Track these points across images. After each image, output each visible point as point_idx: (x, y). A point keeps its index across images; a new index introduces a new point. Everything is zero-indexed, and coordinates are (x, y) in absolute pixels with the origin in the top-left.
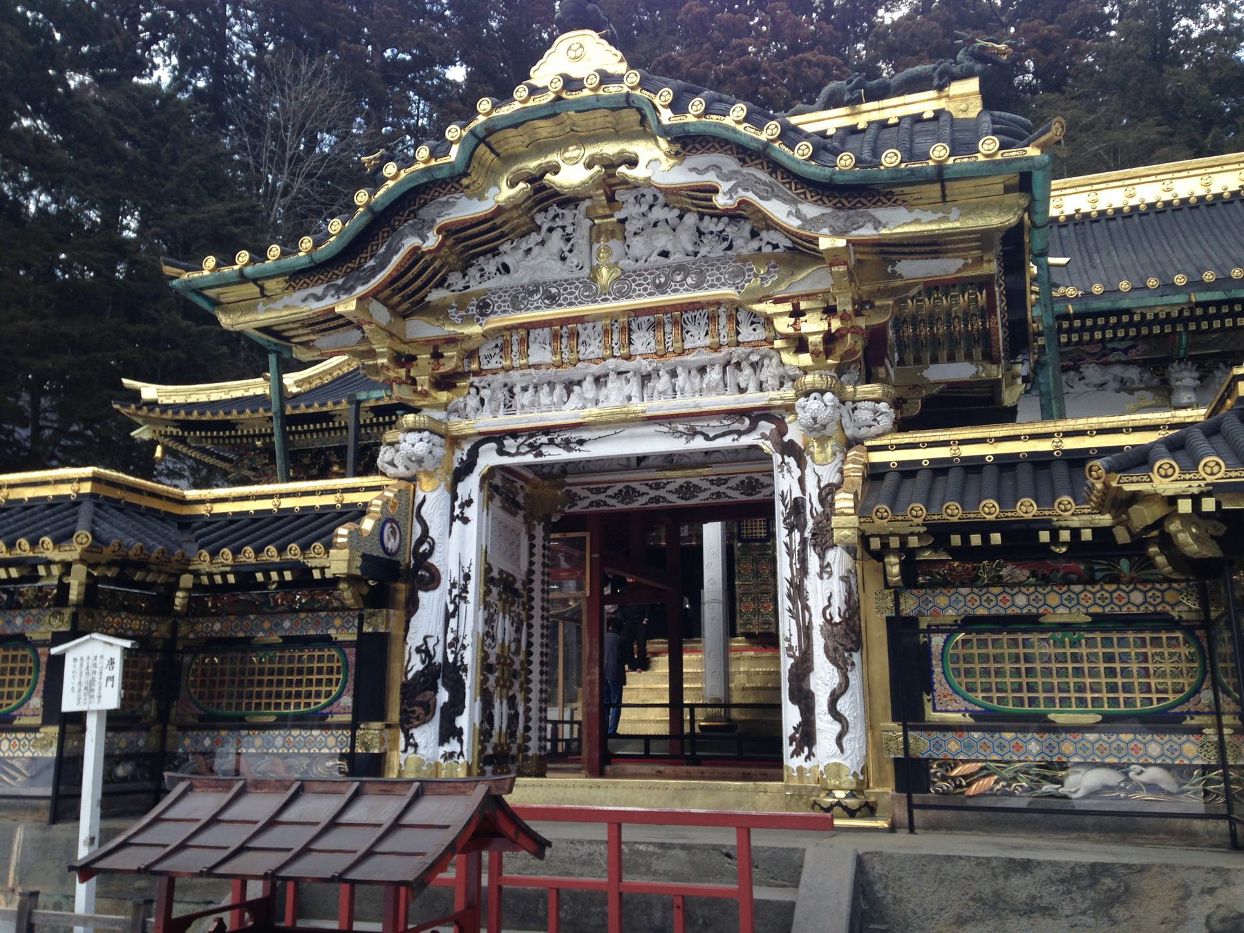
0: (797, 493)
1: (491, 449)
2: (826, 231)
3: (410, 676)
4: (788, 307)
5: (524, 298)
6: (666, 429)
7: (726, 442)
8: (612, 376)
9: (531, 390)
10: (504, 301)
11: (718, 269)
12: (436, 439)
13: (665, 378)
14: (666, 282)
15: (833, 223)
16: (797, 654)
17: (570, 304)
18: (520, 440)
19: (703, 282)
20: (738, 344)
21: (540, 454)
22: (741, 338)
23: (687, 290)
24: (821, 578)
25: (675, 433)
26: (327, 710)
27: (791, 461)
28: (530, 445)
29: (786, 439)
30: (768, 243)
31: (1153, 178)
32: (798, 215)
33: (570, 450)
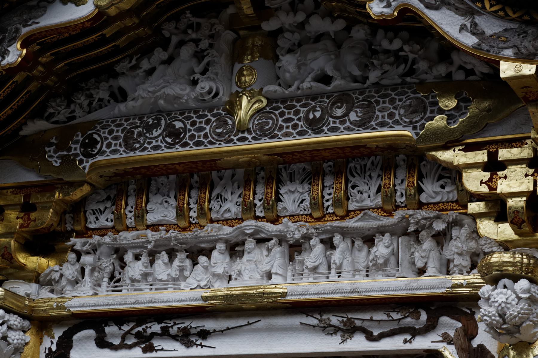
1: (88, 338)
5: (140, 134)
6: (314, 322)
8: (250, 244)
9: (145, 259)
10: (116, 138)
11: (392, 101)
12: (14, 320)
13: (319, 249)
14: (322, 118)
17: (198, 144)
18: (126, 328)
19: (370, 119)
20: (421, 205)
22: (423, 198)
23: (348, 129)
28: (138, 335)
29: (475, 343)
30: (461, 68)
32: (475, 31)
33: (189, 344)
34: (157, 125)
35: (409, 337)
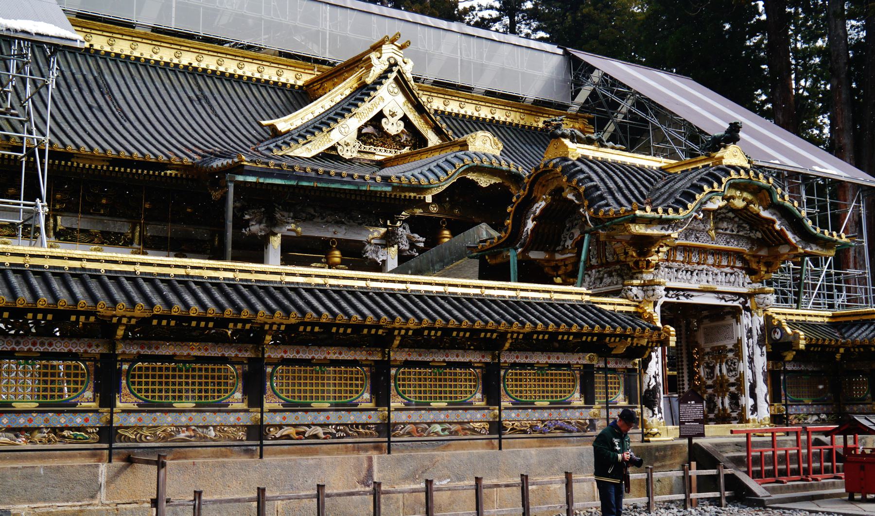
3: (651, 387)
4: (757, 260)
7: (730, 303)
21: (678, 299)
25: (718, 298)
27: (749, 314)
29: (747, 305)
31: (457, 99)
33: (687, 298)
34: (692, 234)
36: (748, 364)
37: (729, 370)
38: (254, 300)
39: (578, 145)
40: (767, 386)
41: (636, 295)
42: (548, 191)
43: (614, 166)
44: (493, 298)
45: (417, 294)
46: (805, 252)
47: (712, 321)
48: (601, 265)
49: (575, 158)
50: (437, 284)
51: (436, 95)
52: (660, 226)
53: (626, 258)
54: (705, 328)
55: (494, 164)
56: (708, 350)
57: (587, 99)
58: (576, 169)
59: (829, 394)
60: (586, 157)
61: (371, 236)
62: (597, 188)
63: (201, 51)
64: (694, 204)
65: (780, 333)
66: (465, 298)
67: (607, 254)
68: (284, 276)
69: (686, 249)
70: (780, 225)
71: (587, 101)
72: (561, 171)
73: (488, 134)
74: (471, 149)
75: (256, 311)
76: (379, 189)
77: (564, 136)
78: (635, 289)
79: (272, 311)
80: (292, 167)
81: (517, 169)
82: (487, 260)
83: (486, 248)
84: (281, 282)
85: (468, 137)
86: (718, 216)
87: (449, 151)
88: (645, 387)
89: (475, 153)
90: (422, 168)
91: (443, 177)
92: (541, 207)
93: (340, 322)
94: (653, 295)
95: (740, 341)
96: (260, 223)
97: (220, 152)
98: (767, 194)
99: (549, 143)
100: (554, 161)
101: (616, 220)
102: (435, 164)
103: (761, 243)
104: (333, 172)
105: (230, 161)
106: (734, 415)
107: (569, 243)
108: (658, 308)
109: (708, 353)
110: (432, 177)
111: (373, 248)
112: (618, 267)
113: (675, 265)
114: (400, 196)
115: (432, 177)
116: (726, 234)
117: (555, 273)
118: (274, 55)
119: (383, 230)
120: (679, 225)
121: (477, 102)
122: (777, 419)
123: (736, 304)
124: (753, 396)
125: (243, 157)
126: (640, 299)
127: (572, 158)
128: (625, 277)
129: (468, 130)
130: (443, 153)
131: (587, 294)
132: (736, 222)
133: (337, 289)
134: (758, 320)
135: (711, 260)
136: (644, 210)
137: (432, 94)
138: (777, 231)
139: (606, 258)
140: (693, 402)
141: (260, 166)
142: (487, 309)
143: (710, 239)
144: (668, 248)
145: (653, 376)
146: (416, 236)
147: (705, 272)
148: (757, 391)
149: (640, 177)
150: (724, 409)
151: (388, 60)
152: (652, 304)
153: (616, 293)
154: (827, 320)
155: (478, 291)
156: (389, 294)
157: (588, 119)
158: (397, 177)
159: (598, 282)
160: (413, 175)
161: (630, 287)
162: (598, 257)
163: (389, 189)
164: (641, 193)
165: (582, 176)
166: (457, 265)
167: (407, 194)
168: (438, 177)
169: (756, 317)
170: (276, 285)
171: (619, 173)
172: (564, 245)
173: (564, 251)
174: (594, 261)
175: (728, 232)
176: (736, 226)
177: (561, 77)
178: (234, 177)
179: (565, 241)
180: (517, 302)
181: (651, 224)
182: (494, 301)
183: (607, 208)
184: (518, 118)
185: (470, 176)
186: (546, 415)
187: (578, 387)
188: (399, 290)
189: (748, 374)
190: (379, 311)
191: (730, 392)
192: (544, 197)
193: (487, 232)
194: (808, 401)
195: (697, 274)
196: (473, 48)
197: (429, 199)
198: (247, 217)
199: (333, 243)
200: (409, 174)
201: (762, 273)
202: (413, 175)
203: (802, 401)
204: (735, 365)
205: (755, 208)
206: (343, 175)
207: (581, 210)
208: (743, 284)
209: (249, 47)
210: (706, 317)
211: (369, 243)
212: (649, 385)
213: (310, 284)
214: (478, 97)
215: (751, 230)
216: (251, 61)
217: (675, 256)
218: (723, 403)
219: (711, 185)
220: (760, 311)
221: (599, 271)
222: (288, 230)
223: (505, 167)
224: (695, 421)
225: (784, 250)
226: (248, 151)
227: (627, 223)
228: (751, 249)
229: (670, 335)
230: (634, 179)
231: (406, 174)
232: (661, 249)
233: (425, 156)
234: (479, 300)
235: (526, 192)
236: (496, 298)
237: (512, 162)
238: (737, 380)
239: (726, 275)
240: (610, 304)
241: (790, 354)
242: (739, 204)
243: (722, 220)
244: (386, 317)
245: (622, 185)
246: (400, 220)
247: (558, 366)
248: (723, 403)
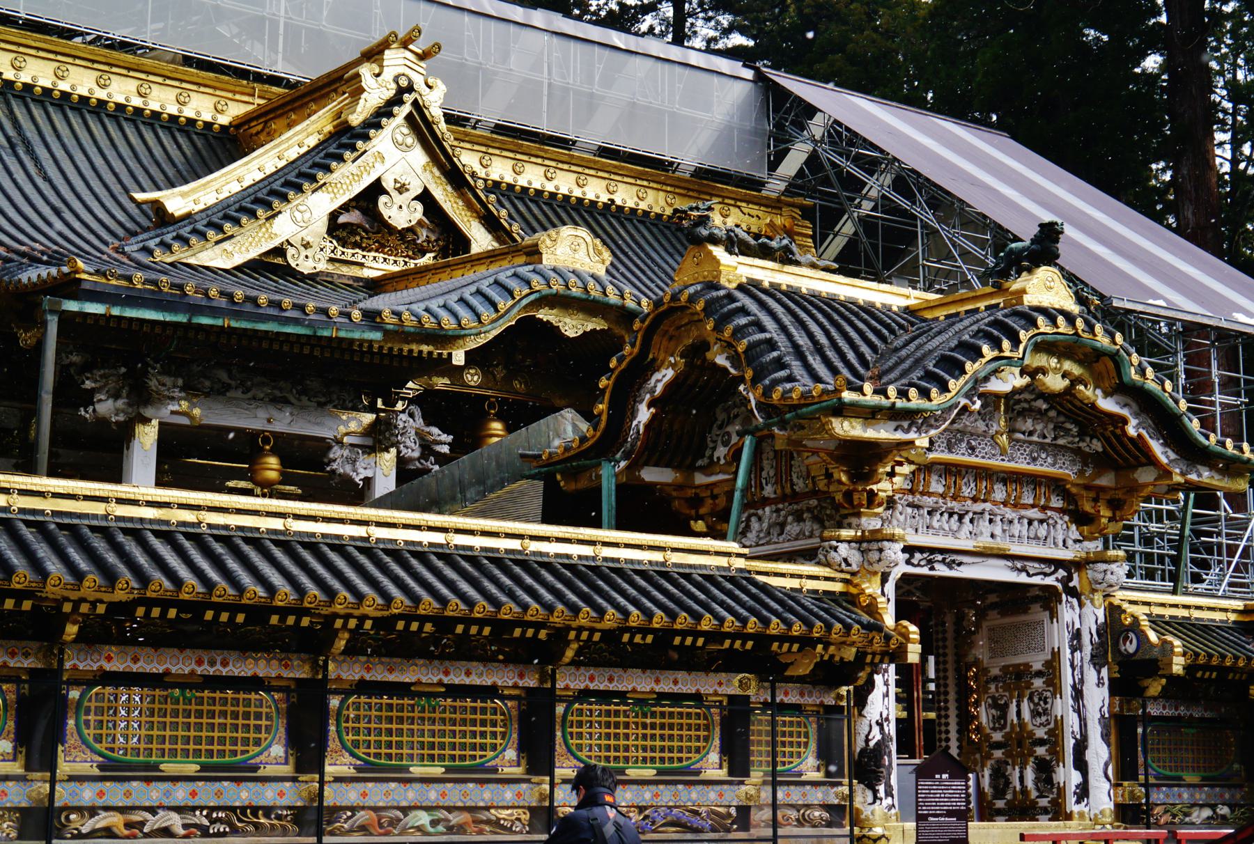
0: (1077, 626)
2: (1178, 471)
3: (872, 744)
4: (1092, 494)
7: (1037, 580)
15: (1181, 466)
16: (1078, 737)
17: (983, 457)
21: (932, 569)
24: (1098, 686)
25: (1014, 569)
26: (257, 760)
27: (1075, 601)
29: (1071, 584)
31: (539, 161)
33: (951, 568)
34: (961, 441)
35: (1042, 576)
36: (1071, 702)
37: (1035, 714)
38: (43, 551)
39: (742, 259)
40: (1109, 745)
41: (845, 560)
42: (681, 348)
43: (811, 303)
44: (546, 559)
45: (389, 546)
46: (1187, 482)
47: (1003, 614)
48: (783, 498)
49: (734, 285)
50: (431, 529)
51: (497, 152)
52: (894, 424)
53: (828, 485)
54: (991, 629)
55: (593, 293)
56: (995, 671)
57: (801, 169)
58: (733, 306)
59: (1236, 766)
60: (756, 284)
61: (342, 429)
62: (771, 344)
63: (22, 49)
64: (962, 381)
65: (1135, 641)
66: (487, 558)
67: (794, 476)
68: (113, 504)
69: (951, 471)
70: (1137, 427)
71: (800, 173)
72: (704, 310)
73: (583, 232)
74: (548, 260)
75: (44, 574)
76: (357, 335)
77: (714, 240)
78: (843, 549)
79: (79, 575)
80: (181, 287)
81: (639, 304)
82: (558, 482)
83: (556, 459)
84: (106, 517)
85: (543, 239)
86: (1015, 404)
87: (505, 264)
88: (860, 744)
89: (554, 270)
90: (447, 297)
91: (487, 314)
92: (665, 380)
93: (220, 600)
94: (880, 560)
95: (1056, 655)
96: (116, 396)
97: (43, 253)
98: (1111, 365)
99: (686, 248)
100: (692, 290)
101: (804, 410)
102: (473, 288)
103: (1101, 462)
104: (263, 299)
105: (54, 271)
106: (1044, 802)
107: (721, 452)
108: (890, 588)
109: (995, 679)
110: (465, 315)
111: (346, 453)
112: (814, 502)
113: (929, 501)
114: (401, 350)
115: (465, 315)
116: (1031, 443)
117: (693, 512)
118: (173, 62)
119: (368, 418)
120: (932, 422)
121: (580, 169)
122: (1128, 813)
123: (1050, 581)
124: (1081, 765)
125: (80, 264)
126: (855, 568)
127: (727, 285)
128: (827, 524)
129: (535, 224)
130: (494, 268)
131: (739, 555)
132: (1051, 420)
133: (223, 533)
134: (1095, 614)
135: (999, 493)
136: (860, 390)
137: (491, 151)
138: (1131, 439)
139: (792, 484)
140: (945, 776)
141: (114, 282)
142: (529, 580)
143: (998, 451)
144: (913, 467)
145: (877, 723)
146: (435, 430)
147: (987, 517)
148: (1090, 756)
149: (861, 325)
150: (1024, 791)
151: (396, 79)
152: (878, 579)
153: (808, 555)
154: (1233, 617)
155: (515, 544)
156: (357, 548)
157: (803, 208)
158: (394, 313)
159: (775, 531)
160: (427, 310)
161: (834, 543)
162: (776, 483)
163: (377, 336)
164: (861, 357)
165: (743, 321)
166: (511, 492)
167: (414, 347)
168: (478, 316)
169: (1088, 608)
170: (95, 523)
171: (820, 316)
172: (711, 456)
173: (708, 469)
174: (769, 491)
175: (1035, 438)
176: (1051, 426)
177: (749, 124)
178: (60, 304)
179: (714, 449)
180: (594, 569)
181: (873, 418)
182: (548, 566)
183: (788, 386)
184: (662, 203)
185: (544, 315)
186: (648, 796)
187: (717, 742)
188: (352, 538)
189: (1072, 721)
190: (304, 580)
191: (1036, 758)
192: (672, 359)
193: (575, 426)
194: (1191, 778)
195: (972, 521)
196: (575, 61)
197: (459, 358)
198: (88, 384)
199: (266, 440)
200: (419, 308)
201: (1104, 521)
202: (427, 310)
203: (1180, 778)
204: (1046, 703)
205: (1088, 392)
206: (284, 306)
207: (741, 388)
208: (1064, 541)
209: (124, 46)
210: (993, 606)
211: (339, 442)
212: (867, 740)
213: (167, 523)
214: (582, 159)
215: (1082, 435)
216: (124, 72)
217: (927, 484)
218: (1022, 779)
219: (997, 344)
220: (1098, 597)
221: (778, 511)
222: (173, 412)
223: (613, 298)
224: (950, 813)
225: (1145, 476)
226: (103, 253)
227: (826, 416)
228: (1081, 473)
229: (908, 640)
230: (848, 329)
231: (414, 307)
232: (898, 469)
233: (460, 272)
234: (516, 562)
235: (636, 350)
236: (552, 560)
237: (628, 289)
238: (1051, 733)
239: (1030, 523)
240: (792, 576)
241: (1155, 684)
242: (1055, 383)
243: (1023, 414)
244: (316, 593)
245: (823, 340)
246: (403, 399)
247: (677, 699)
248: (1022, 779)
